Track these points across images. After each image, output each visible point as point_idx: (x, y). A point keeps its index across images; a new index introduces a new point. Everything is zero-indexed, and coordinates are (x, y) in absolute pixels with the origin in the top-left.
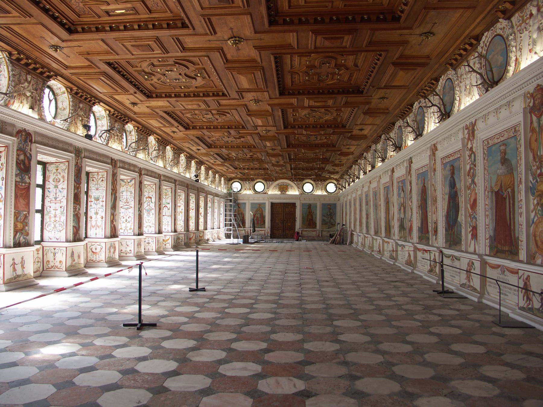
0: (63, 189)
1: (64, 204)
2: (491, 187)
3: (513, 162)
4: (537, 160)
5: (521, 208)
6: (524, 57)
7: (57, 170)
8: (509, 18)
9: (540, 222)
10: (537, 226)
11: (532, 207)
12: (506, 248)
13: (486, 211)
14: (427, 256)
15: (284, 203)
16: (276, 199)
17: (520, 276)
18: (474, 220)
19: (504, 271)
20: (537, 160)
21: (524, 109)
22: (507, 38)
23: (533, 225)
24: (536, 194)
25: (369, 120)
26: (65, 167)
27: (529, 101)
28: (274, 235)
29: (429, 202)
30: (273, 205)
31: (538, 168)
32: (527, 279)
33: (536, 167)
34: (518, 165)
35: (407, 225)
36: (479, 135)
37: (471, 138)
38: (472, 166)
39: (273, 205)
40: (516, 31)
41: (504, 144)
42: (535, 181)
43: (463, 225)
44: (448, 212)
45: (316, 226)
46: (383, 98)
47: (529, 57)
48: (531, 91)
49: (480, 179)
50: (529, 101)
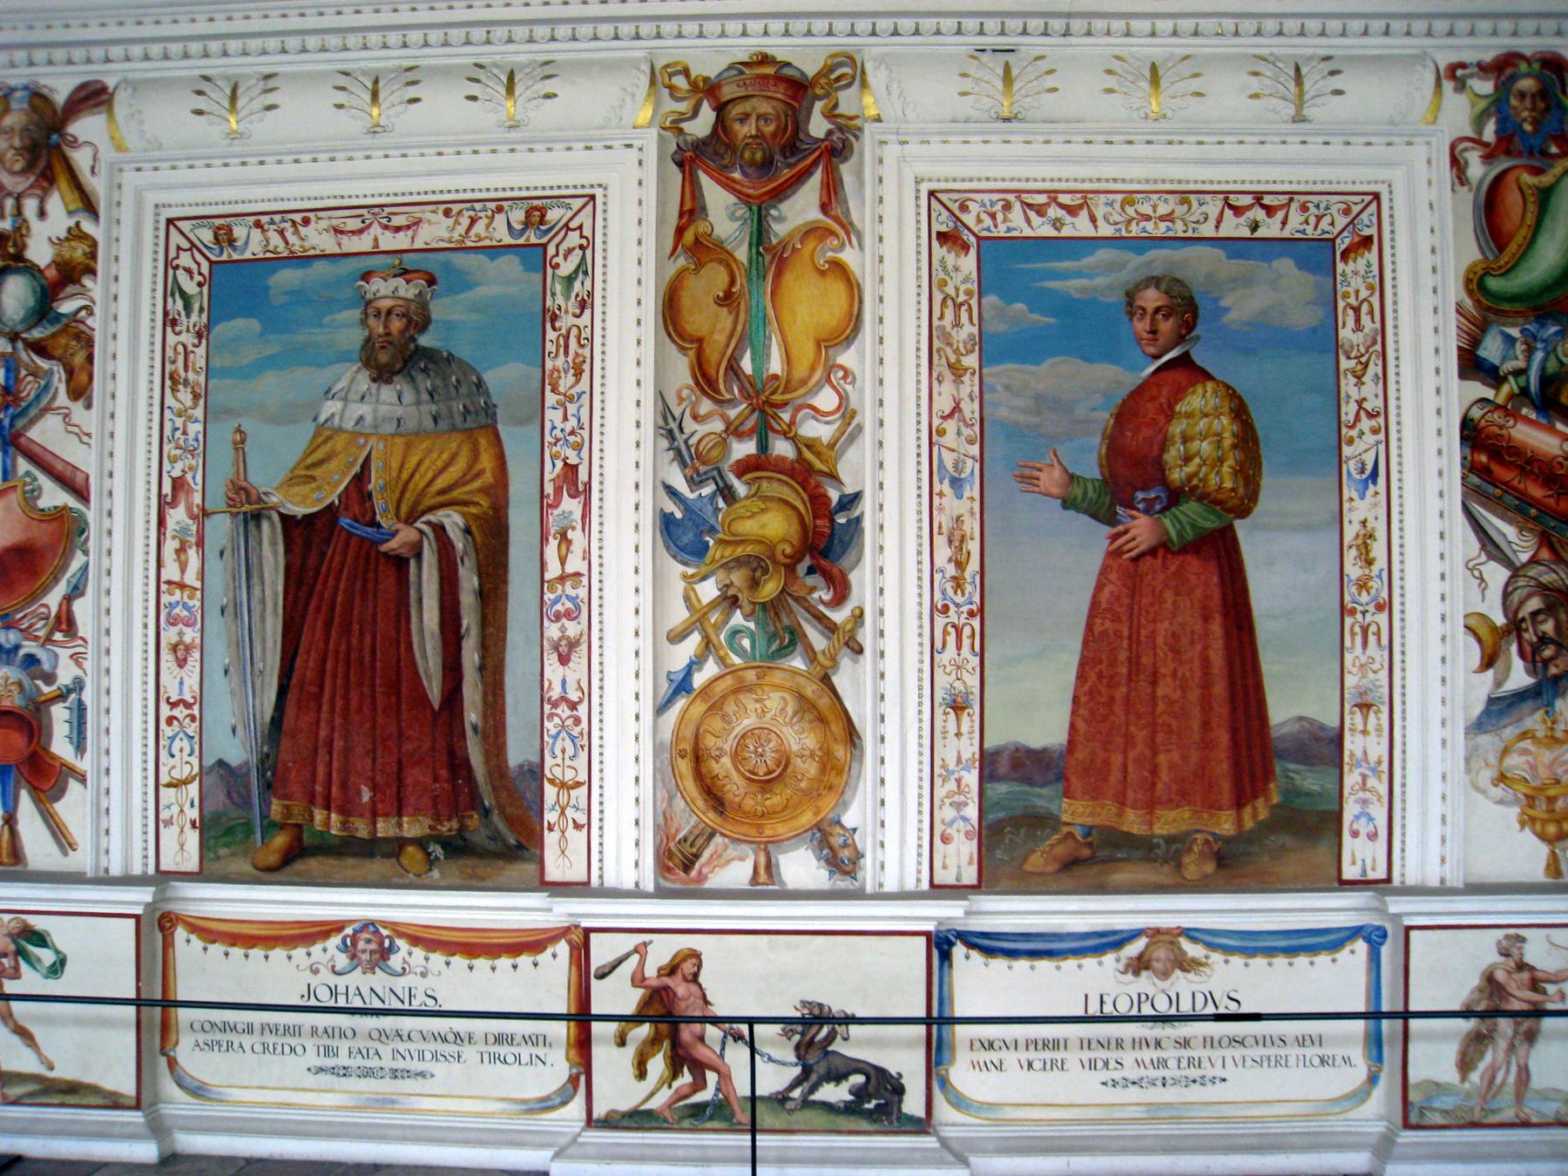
9: (741, 688)
10: (715, 707)
11: (679, 614)
12: (413, 827)
13: (162, 616)
23: (681, 703)
24: (715, 552)
31: (734, 431)
33: (718, 426)
34: (551, 399)
41: (404, 273)
42: (708, 490)
48: (709, 65)
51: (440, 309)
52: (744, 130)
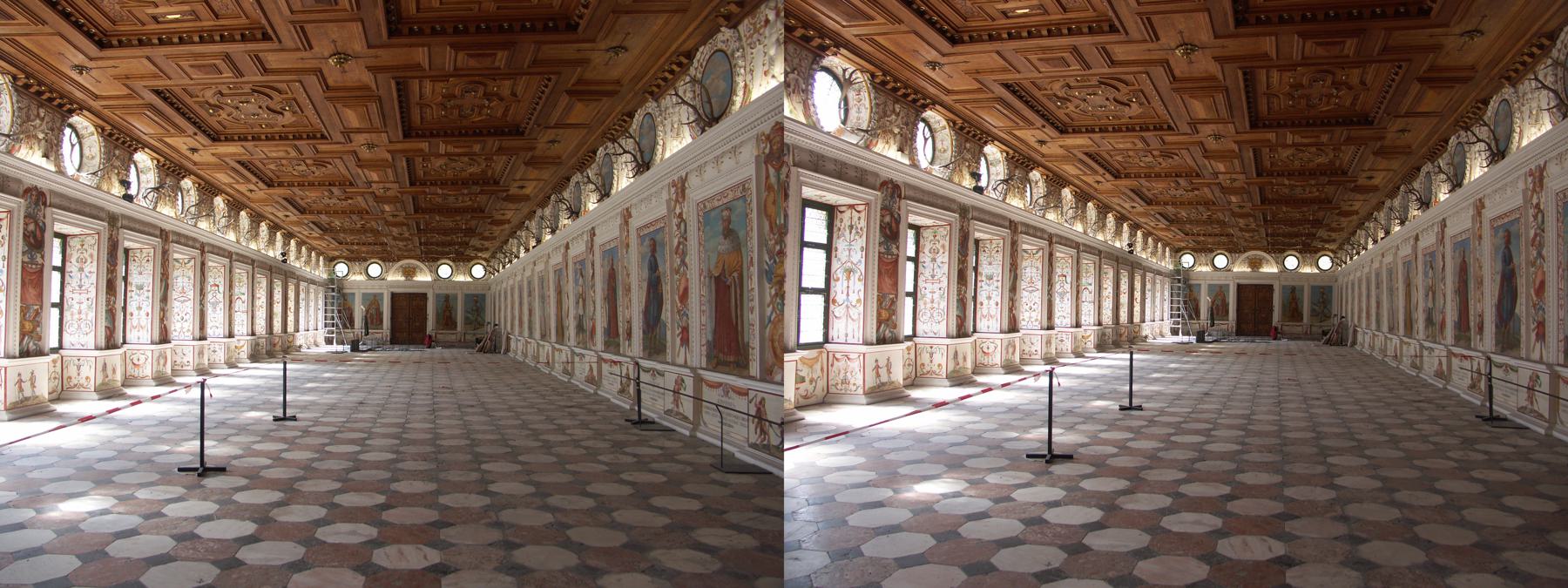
0: (90, 272)
1: (93, 294)
2: (709, 270)
3: (741, 234)
4: (775, 231)
5: (752, 300)
6: (757, 82)
7: (82, 245)
8: (735, 27)
11: (768, 299)
12: (731, 359)
14: (616, 369)
15: (410, 294)
16: (399, 287)
17: (750, 398)
18: (685, 318)
19: (728, 392)
20: (775, 231)
21: (757, 157)
22: (733, 55)
25: (533, 173)
26: (93, 242)
27: (763, 145)
28: (396, 339)
29: (620, 292)
30: (394, 296)
31: (776, 243)
32: (760, 403)
33: (773, 242)
35: (587, 325)
36: (691, 196)
37: (680, 200)
38: (681, 240)
39: (394, 296)
40: (745, 45)
43: (669, 325)
44: (647, 306)
45: (455, 327)
46: (553, 142)
47: (764, 83)
48: (767, 132)
49: (693, 259)
50: (763, 145)
51: (733, 218)
52: (775, 147)
